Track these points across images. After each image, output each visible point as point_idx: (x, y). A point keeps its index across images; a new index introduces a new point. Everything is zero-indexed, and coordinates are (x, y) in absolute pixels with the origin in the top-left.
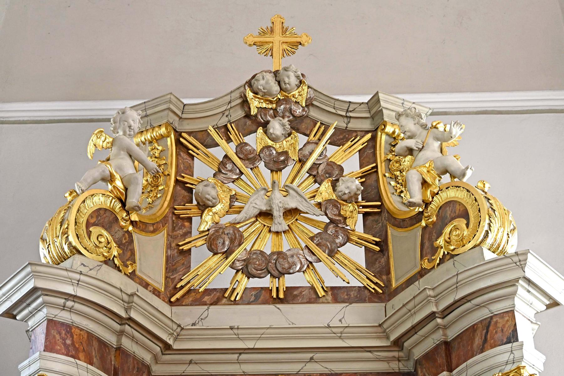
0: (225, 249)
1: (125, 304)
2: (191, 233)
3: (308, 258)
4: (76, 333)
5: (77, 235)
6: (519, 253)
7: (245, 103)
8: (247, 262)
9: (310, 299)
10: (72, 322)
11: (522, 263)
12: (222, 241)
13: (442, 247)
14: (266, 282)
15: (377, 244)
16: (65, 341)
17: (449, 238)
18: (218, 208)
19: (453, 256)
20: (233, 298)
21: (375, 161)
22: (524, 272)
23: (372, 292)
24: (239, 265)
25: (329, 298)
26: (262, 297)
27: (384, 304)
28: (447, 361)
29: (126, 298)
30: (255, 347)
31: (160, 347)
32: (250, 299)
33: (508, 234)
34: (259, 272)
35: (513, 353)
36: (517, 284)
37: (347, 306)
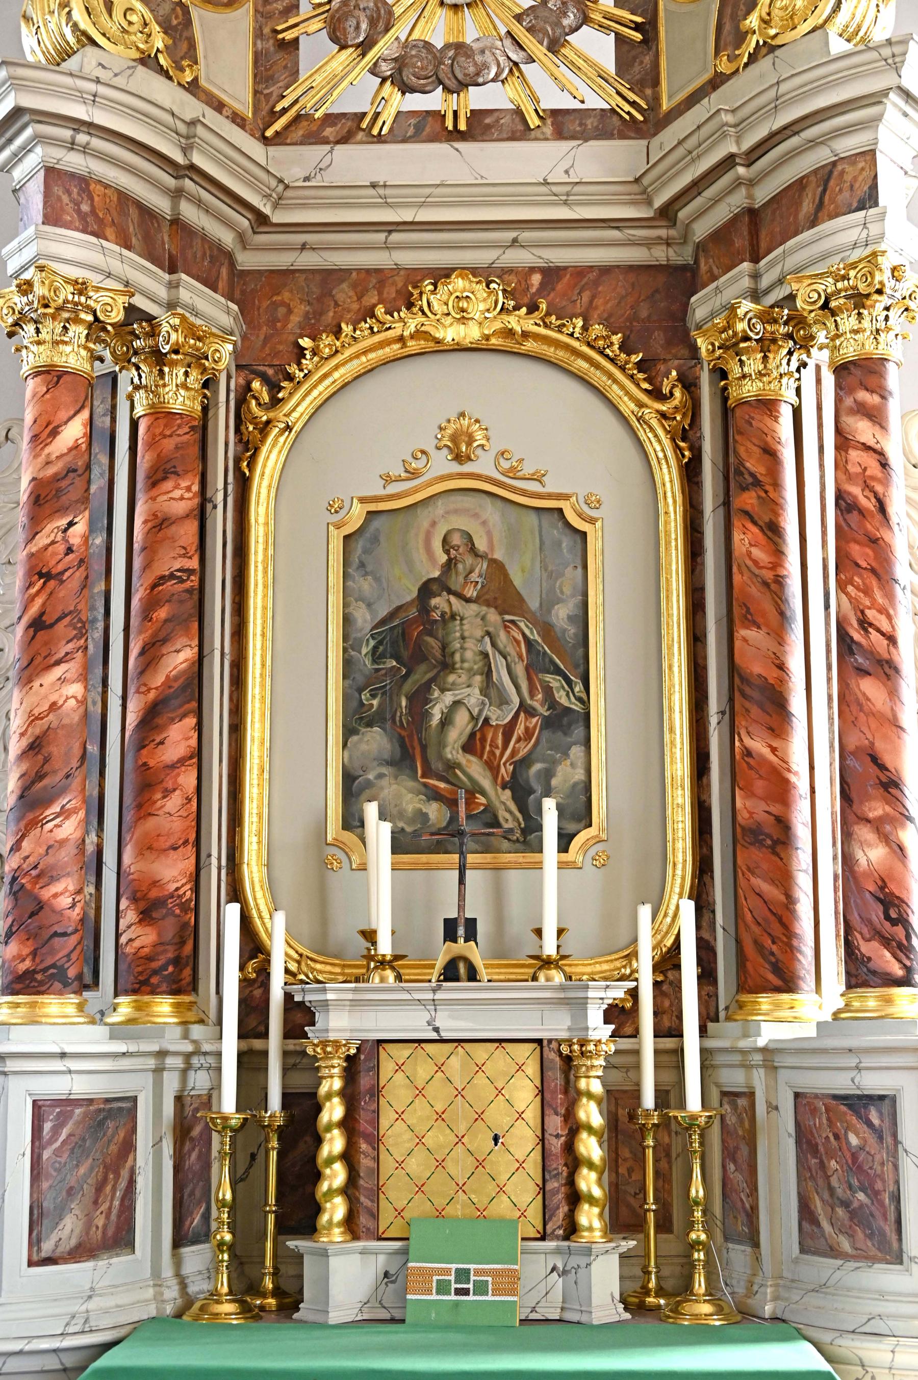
0: (361, 39)
1: (182, 140)
2: (297, 7)
3: (511, 55)
4: (97, 193)
5: (87, 8)
6: (893, 40)
8: (400, 62)
9: (513, 132)
10: (89, 173)
11: (897, 59)
12: (355, 22)
13: (754, 32)
14: (434, 100)
15: (637, 27)
16: (79, 206)
17: (769, 14)
19: (773, 49)
20: (375, 132)
22: (900, 77)
23: (626, 120)
24: (386, 69)
25: (548, 130)
26: (428, 129)
27: (645, 142)
28: (751, 245)
29: (182, 128)
30: (416, 220)
31: (249, 219)
32: (407, 132)
33: (877, 6)
34: (422, 82)
35: (867, 228)
36: (885, 100)
37: (579, 145)
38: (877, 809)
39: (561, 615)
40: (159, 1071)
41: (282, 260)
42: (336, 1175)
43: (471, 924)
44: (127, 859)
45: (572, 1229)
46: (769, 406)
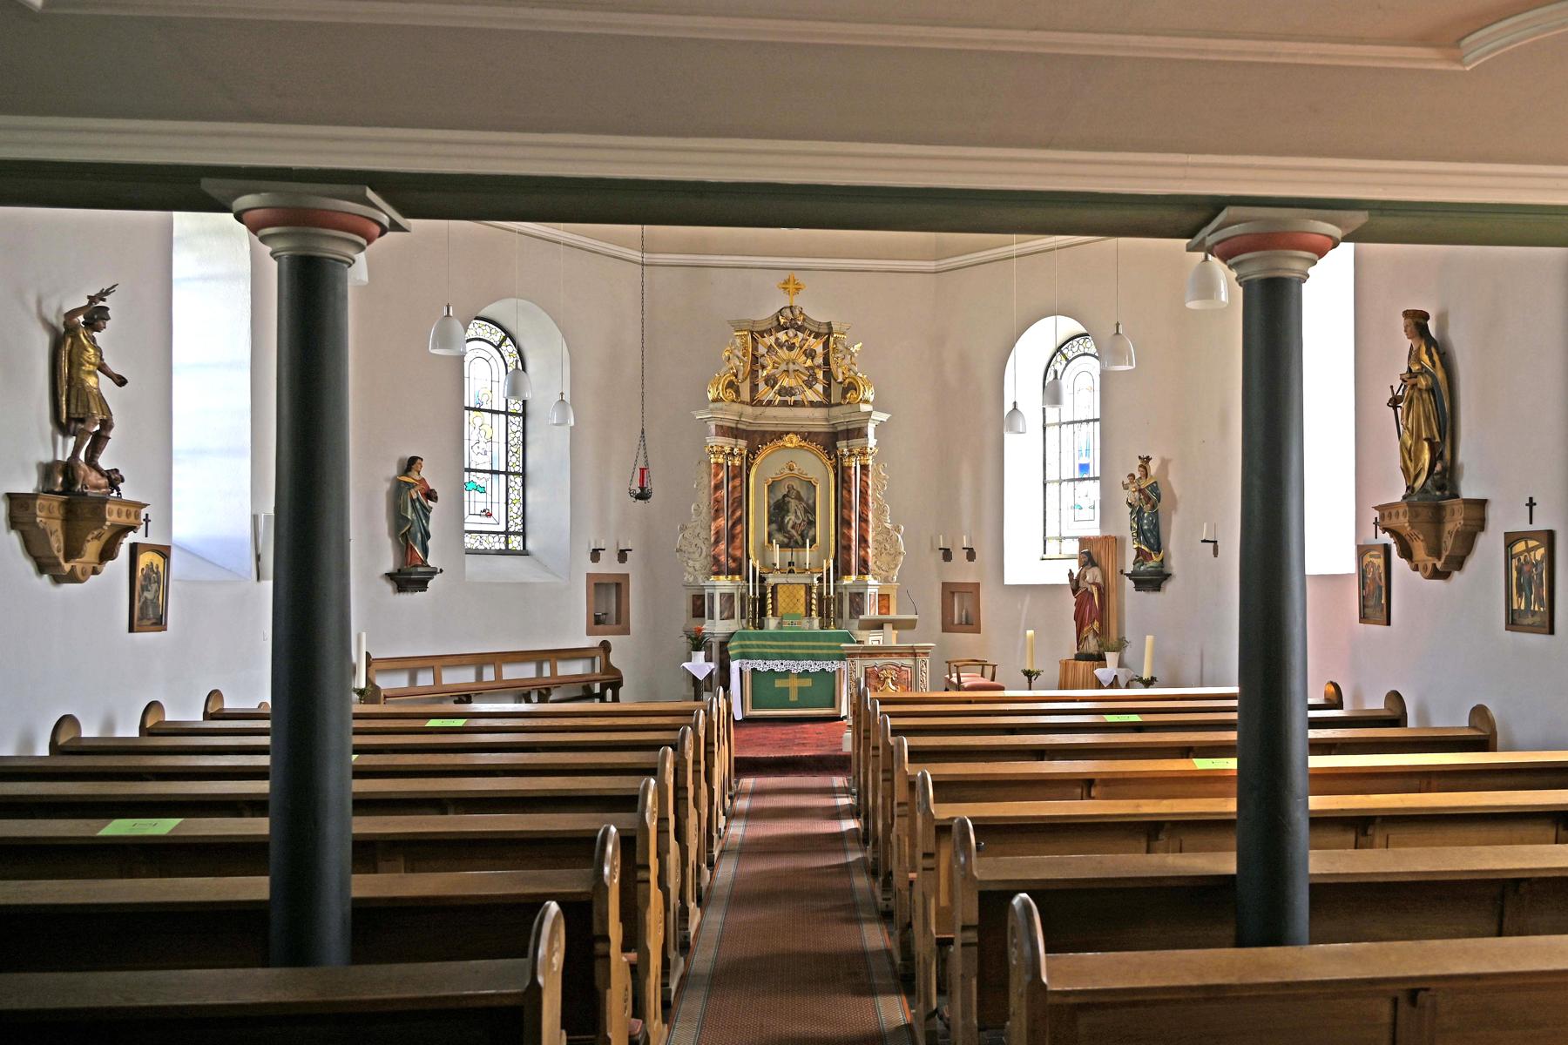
7: (778, 320)
18: (769, 368)
21: (829, 348)
38: (863, 545)
39: (811, 502)
40: (738, 589)
41: (755, 429)
42: (770, 606)
43: (793, 563)
44: (730, 550)
45: (811, 615)
46: (850, 468)
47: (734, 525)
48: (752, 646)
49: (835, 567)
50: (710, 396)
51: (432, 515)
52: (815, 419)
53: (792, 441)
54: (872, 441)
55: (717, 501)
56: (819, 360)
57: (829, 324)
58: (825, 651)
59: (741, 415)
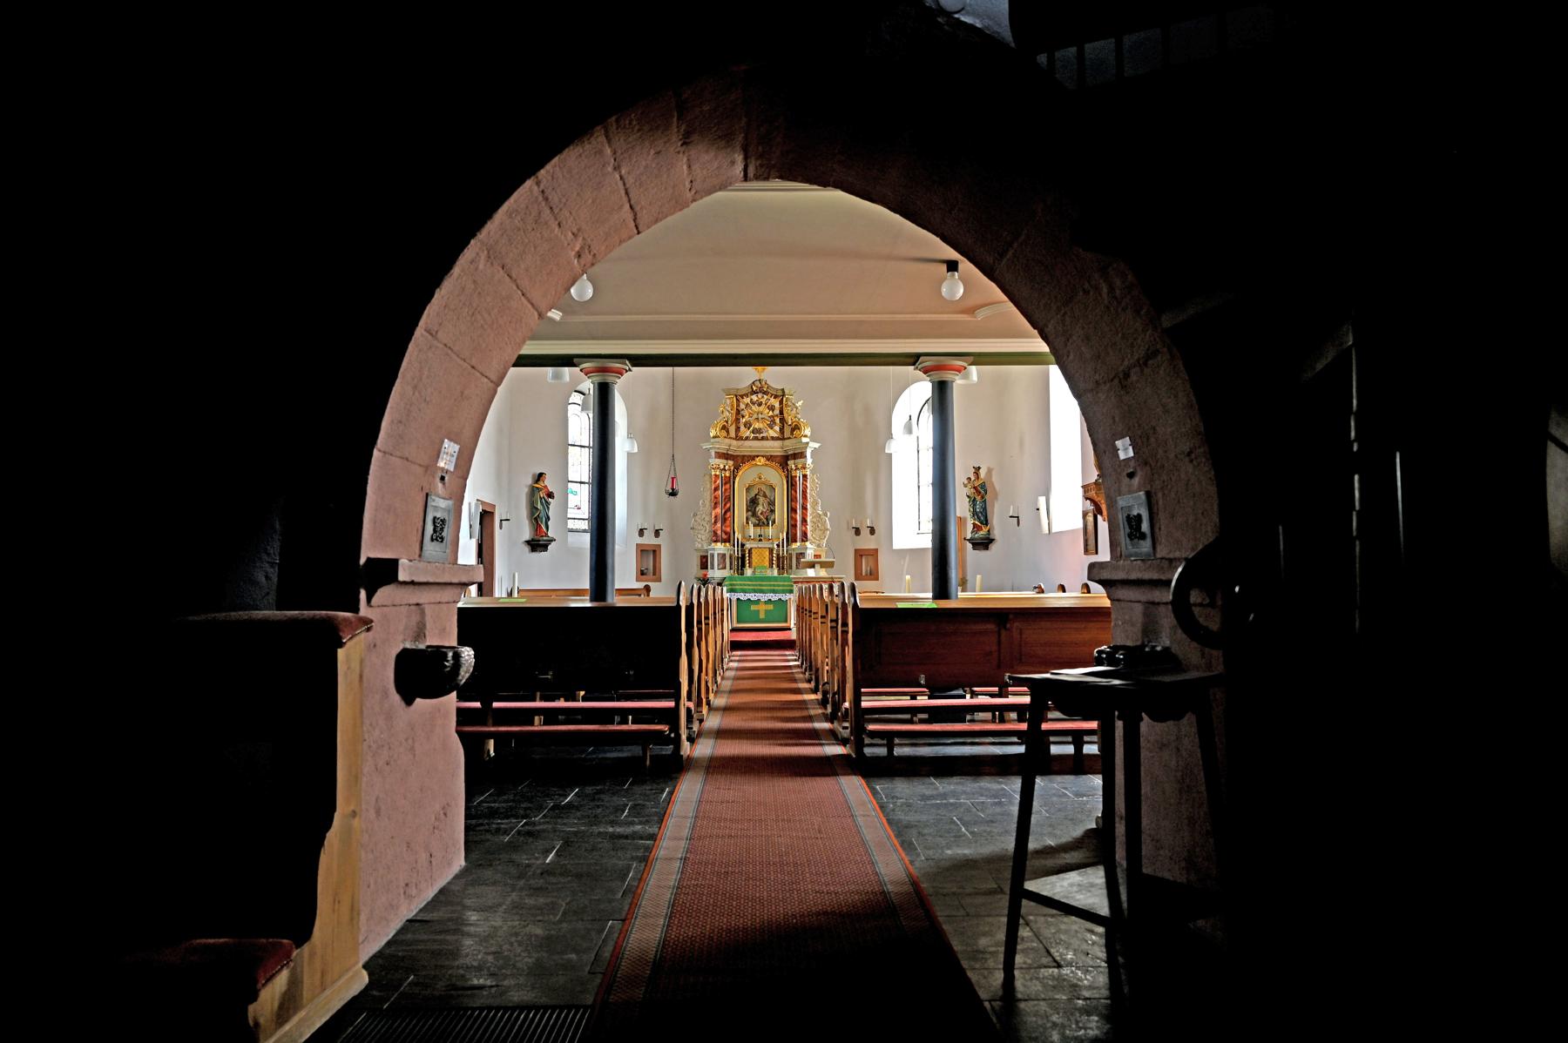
46: (796, 477)
47: (726, 512)
48: (737, 585)
49: (787, 538)
50: (712, 435)
51: (550, 507)
52: (775, 448)
53: (761, 461)
54: (809, 460)
55: (715, 498)
56: (777, 412)
57: (783, 390)
58: (781, 588)
59: (730, 446)
